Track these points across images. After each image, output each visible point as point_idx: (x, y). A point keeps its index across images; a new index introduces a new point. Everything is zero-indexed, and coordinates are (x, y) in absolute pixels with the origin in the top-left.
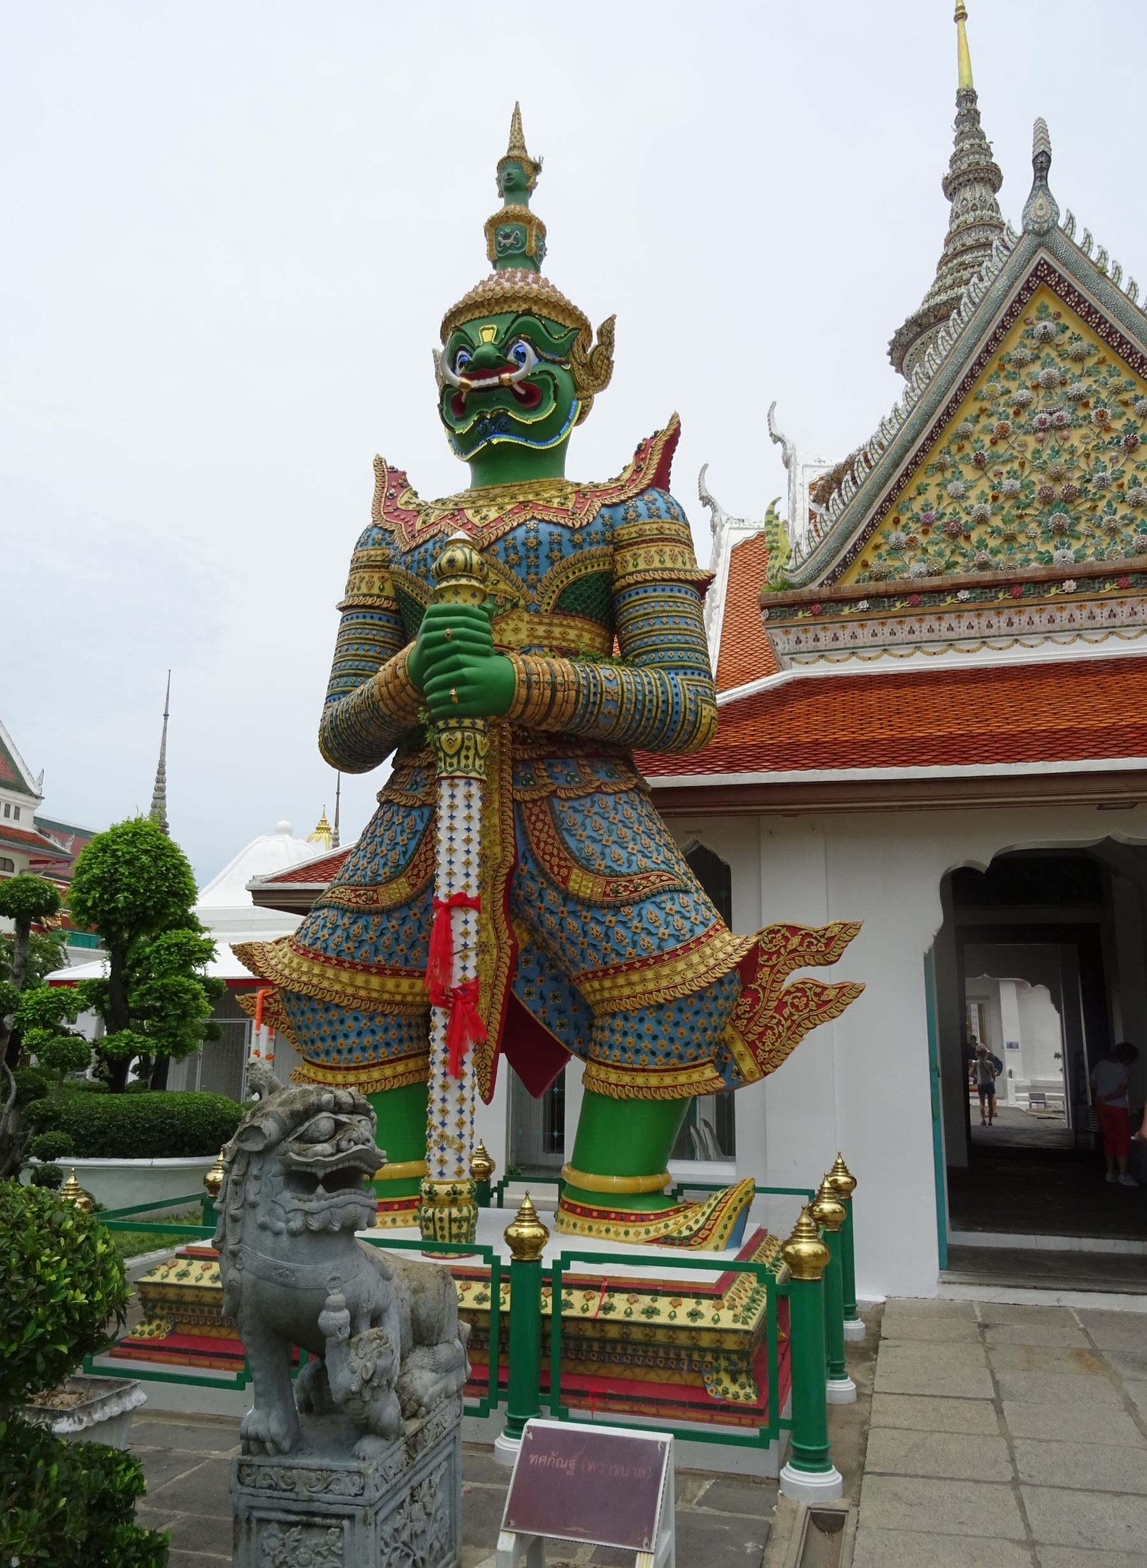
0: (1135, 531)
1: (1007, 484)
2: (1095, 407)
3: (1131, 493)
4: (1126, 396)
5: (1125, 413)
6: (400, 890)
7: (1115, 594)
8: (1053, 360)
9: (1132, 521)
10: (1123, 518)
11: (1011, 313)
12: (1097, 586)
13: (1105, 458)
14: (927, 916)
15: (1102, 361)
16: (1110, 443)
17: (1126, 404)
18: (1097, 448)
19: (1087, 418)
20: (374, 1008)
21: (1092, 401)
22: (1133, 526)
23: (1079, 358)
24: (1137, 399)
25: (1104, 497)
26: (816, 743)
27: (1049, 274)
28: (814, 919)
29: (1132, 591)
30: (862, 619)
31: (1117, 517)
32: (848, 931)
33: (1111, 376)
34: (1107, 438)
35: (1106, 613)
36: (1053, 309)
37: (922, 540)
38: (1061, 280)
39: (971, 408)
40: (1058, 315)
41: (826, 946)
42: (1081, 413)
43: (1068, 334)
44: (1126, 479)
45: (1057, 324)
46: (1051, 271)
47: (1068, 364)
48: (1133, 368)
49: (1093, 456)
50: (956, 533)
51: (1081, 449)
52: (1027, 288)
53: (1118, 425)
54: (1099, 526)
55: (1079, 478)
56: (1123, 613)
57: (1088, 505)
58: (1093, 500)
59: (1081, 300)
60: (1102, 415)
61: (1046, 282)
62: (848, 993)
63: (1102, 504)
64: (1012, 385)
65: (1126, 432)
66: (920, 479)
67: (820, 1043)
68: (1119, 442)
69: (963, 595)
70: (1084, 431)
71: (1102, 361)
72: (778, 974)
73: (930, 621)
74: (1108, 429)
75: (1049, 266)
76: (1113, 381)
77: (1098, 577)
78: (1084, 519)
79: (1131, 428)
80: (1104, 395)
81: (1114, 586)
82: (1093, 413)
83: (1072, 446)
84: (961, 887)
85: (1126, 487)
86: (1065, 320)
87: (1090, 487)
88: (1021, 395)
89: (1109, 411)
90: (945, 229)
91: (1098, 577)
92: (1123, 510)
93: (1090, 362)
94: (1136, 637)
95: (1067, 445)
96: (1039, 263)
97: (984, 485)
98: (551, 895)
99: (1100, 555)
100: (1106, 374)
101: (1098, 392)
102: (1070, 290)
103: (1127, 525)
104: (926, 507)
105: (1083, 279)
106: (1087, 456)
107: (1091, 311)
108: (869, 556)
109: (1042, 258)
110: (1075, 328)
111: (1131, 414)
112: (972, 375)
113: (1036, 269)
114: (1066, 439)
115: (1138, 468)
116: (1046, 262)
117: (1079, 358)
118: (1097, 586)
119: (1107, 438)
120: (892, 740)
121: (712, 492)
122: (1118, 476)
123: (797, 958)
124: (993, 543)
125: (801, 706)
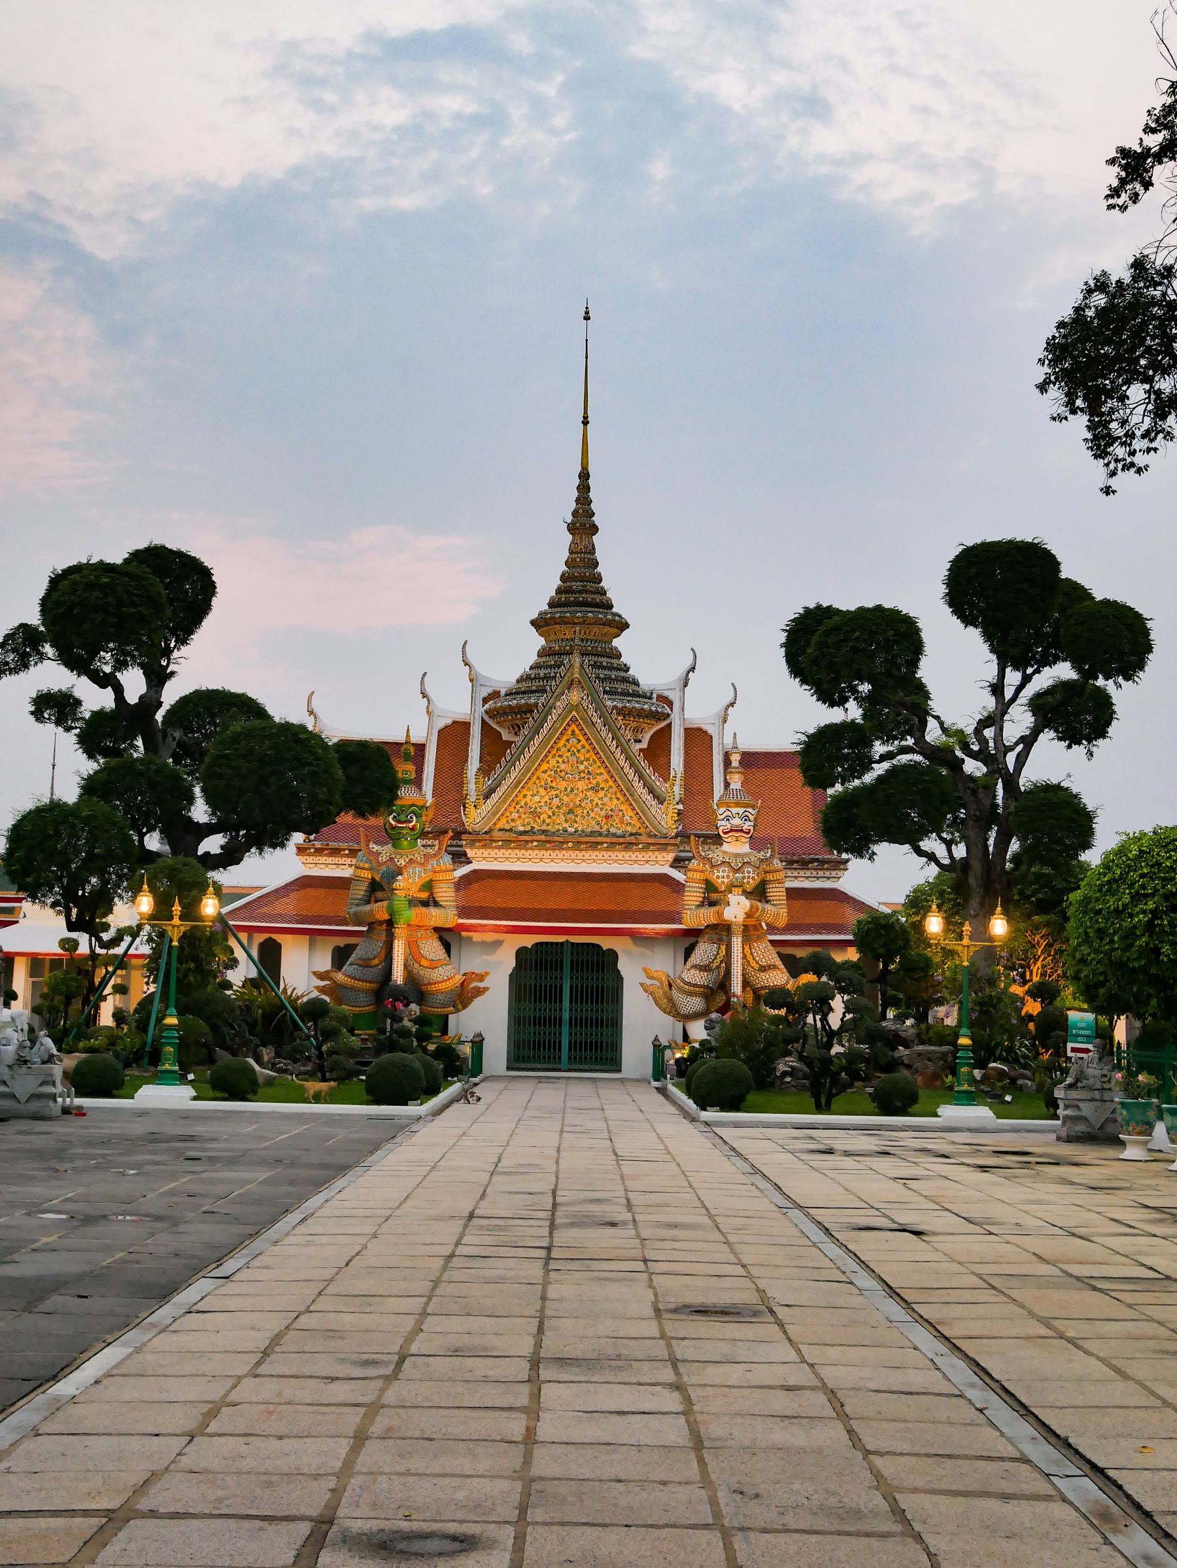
1: (556, 801)
6: (376, 961)
11: (561, 734)
14: (511, 963)
20: (366, 991)
26: (481, 907)
28: (478, 971)
30: (500, 848)
32: (487, 973)
36: (577, 732)
37: (523, 816)
39: (545, 767)
41: (481, 978)
50: (535, 814)
52: (568, 725)
53: (594, 782)
62: (486, 989)
64: (560, 760)
66: (525, 792)
67: (477, 1002)
69: (535, 843)
72: (469, 984)
73: (523, 851)
79: (598, 784)
84: (521, 953)
88: (563, 766)
90: (566, 555)
97: (547, 798)
98: (416, 965)
104: (526, 804)
107: (588, 739)
108: (504, 820)
110: (583, 741)
111: (599, 779)
112: (546, 756)
120: (504, 909)
121: (429, 692)
123: (473, 980)
124: (548, 821)
125: (475, 886)
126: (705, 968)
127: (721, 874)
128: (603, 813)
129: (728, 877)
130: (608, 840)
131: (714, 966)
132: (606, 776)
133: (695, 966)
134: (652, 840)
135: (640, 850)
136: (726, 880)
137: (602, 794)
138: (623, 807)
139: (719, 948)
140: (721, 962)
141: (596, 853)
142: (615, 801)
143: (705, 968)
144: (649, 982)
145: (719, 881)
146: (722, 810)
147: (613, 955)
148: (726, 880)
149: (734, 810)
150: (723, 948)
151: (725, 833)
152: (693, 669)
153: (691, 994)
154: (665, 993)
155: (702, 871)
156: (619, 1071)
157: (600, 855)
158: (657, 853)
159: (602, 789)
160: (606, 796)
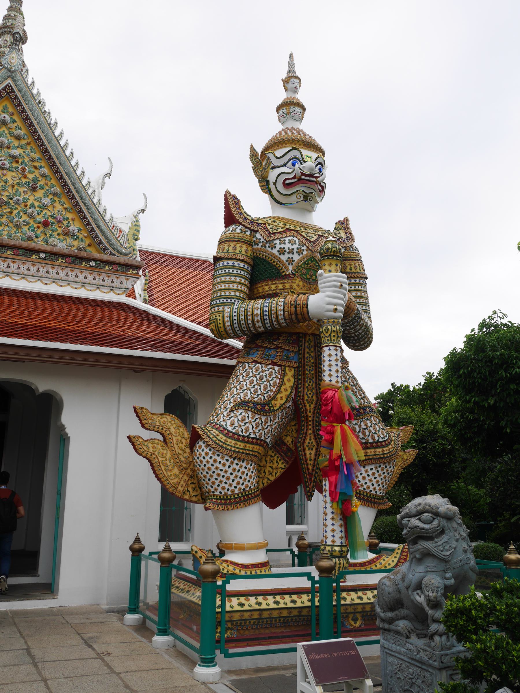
0: (29, 229)
2: (22, 165)
3: (30, 210)
4: (37, 164)
5: (34, 172)
7: (11, 256)
8: (6, 134)
9: (28, 224)
10: (24, 221)
12: (3, 250)
13: (21, 190)
15: (28, 144)
16: (25, 184)
17: (36, 168)
18: (18, 184)
19: (17, 168)
21: (20, 161)
22: (28, 227)
23: (18, 138)
24: (41, 167)
25: (17, 209)
27: (11, 92)
29: (20, 257)
31: (21, 220)
33: (32, 152)
34: (24, 181)
35: (6, 265)
36: (11, 110)
38: (16, 97)
40: (12, 114)
42: (14, 165)
43: (16, 125)
44: (29, 204)
45: (11, 118)
46: (13, 91)
47: (13, 139)
48: (42, 152)
49: (16, 187)
51: (11, 182)
53: (30, 176)
54: (12, 222)
55: (7, 196)
56: (14, 267)
57: (9, 210)
58: (11, 209)
59: (24, 111)
60: (23, 169)
61: (10, 95)
63: (15, 212)
65: (33, 181)
68: (29, 185)
70: (14, 174)
71: (28, 144)
74: (25, 177)
75: (12, 89)
76: (32, 155)
77: (5, 246)
78: (6, 216)
79: (35, 180)
80: (27, 160)
81: (12, 253)
82: (20, 167)
83: (7, 179)
85: (28, 207)
86: (15, 117)
87: (11, 202)
89: (27, 169)
91: (5, 246)
92: (25, 218)
93: (23, 142)
94: (19, 280)
95: (4, 178)
96: (7, 85)
99: (9, 236)
100: (29, 151)
101: (24, 158)
102: (20, 104)
103: (25, 225)
105: (27, 101)
106: (13, 187)
107: (27, 118)
109: (9, 83)
110: (19, 123)
113: (6, 87)
114: (4, 175)
115: (35, 200)
116: (11, 86)
117: (18, 138)
118: (3, 250)
119: (24, 181)
122: (25, 201)
126: (262, 408)
127: (287, 246)
128: (40, 218)
129: (299, 252)
130: (48, 248)
131: (278, 403)
132: (46, 170)
133: (244, 404)
134: (105, 257)
135: (91, 269)
136: (296, 257)
137: (40, 193)
138: (70, 216)
139: (284, 374)
140: (288, 397)
141: (28, 265)
142: (58, 207)
143: (262, 408)
144: (146, 435)
145: (284, 258)
146: (279, 153)
147: (50, 404)
148: (296, 257)
149: (306, 152)
150: (290, 374)
151: (286, 185)
152: (109, 175)
153: (238, 456)
154: (175, 456)
155: (250, 243)
156: (49, 588)
157: (33, 270)
158: (113, 277)
159: (42, 188)
160: (46, 195)
